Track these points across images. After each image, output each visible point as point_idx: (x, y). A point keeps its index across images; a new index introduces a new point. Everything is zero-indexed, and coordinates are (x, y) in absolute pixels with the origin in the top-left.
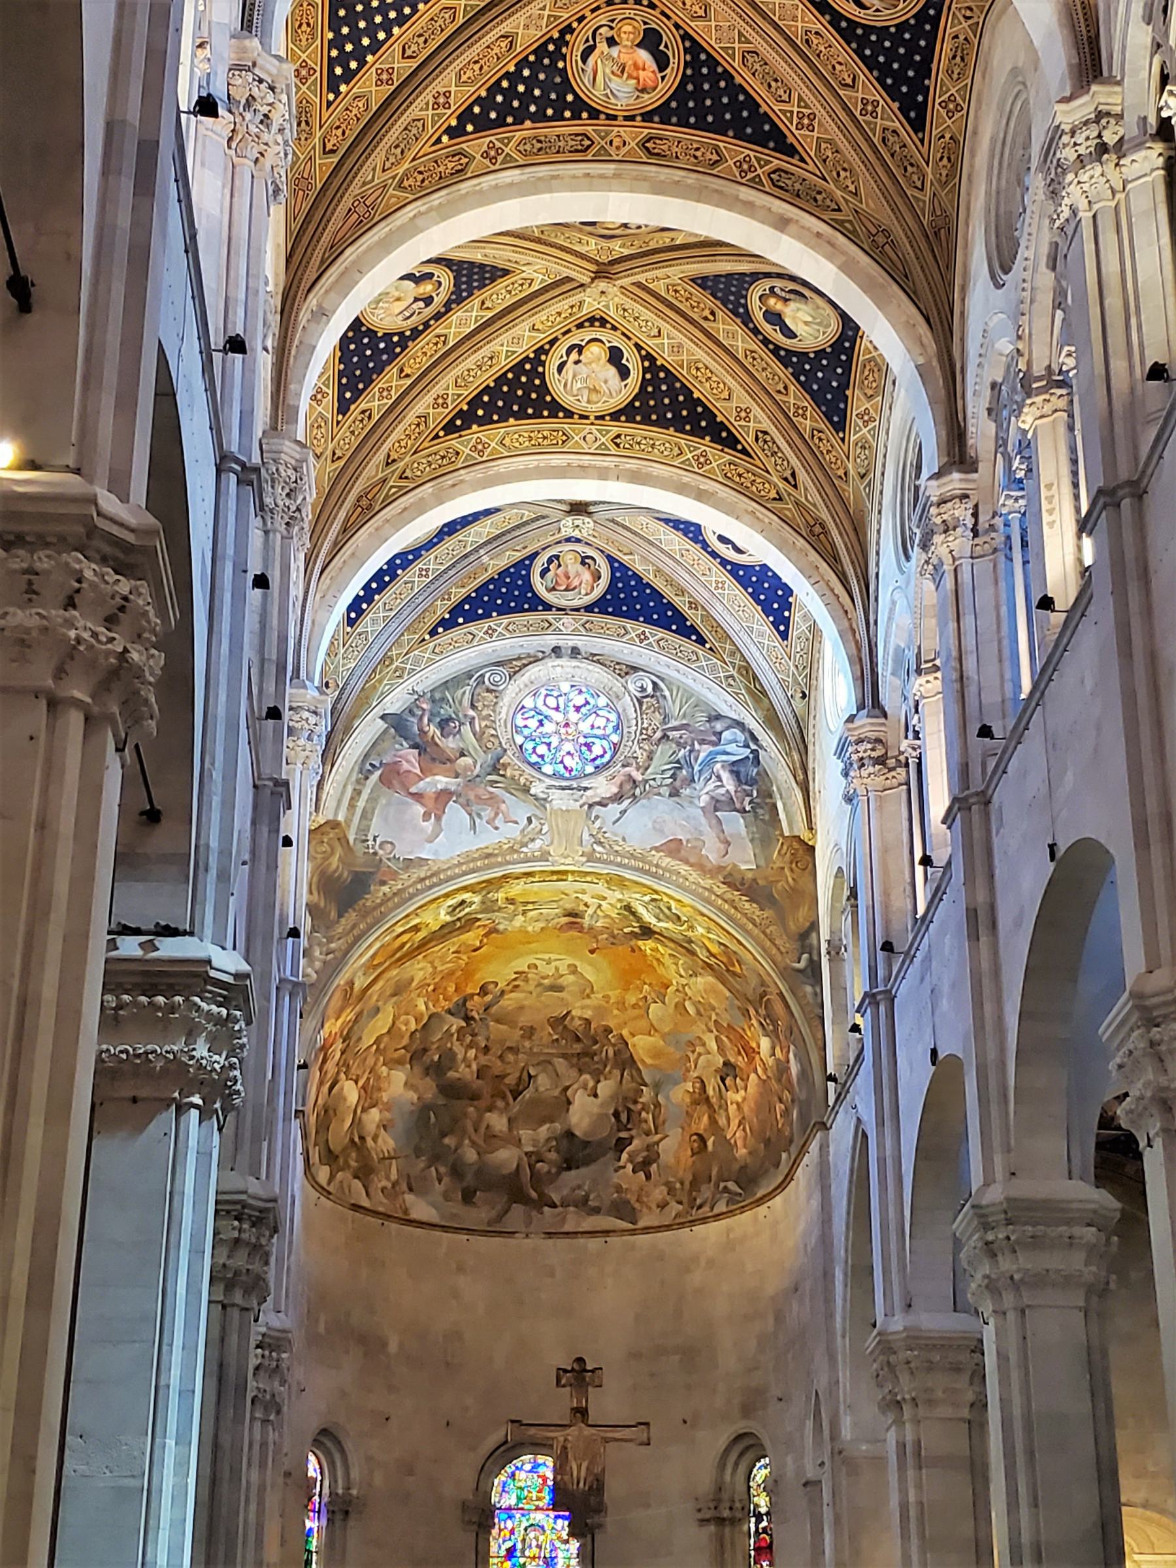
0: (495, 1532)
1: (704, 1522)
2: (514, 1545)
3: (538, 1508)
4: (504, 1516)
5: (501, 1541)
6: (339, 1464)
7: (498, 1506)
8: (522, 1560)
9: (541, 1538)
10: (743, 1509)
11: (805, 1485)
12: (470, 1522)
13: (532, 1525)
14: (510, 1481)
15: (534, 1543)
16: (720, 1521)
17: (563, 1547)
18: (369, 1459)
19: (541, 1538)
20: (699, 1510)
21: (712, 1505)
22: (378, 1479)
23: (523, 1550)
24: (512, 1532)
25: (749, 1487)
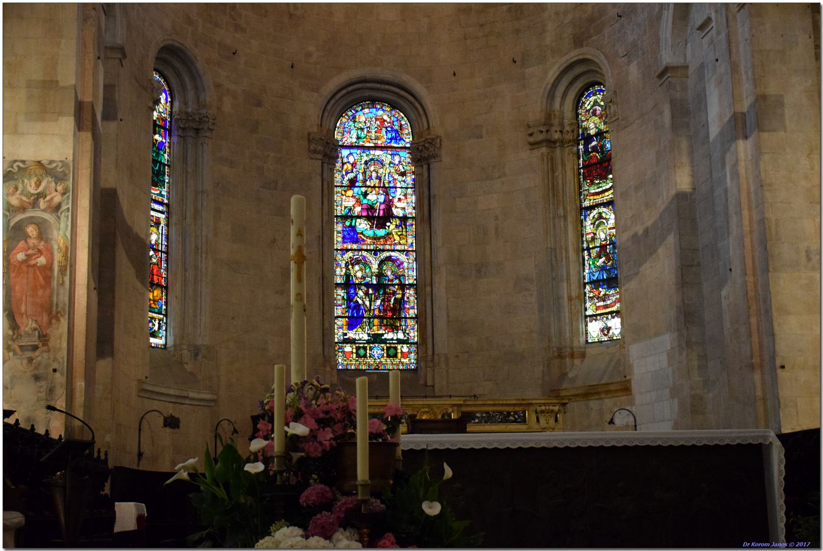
0: (338, 165)
1: (534, 145)
2: (356, 177)
3: (376, 147)
4: (345, 152)
5: (344, 173)
6: (189, 86)
7: (340, 143)
8: (363, 189)
9: (381, 171)
10: (573, 131)
11: (661, 75)
12: (315, 151)
13: (372, 159)
14: (351, 123)
15: (374, 175)
16: (551, 143)
17: (400, 178)
18: (218, 86)
19: (381, 171)
20: (531, 135)
21: (544, 129)
22: (227, 105)
23: (365, 181)
24: (354, 165)
25: (577, 115)
